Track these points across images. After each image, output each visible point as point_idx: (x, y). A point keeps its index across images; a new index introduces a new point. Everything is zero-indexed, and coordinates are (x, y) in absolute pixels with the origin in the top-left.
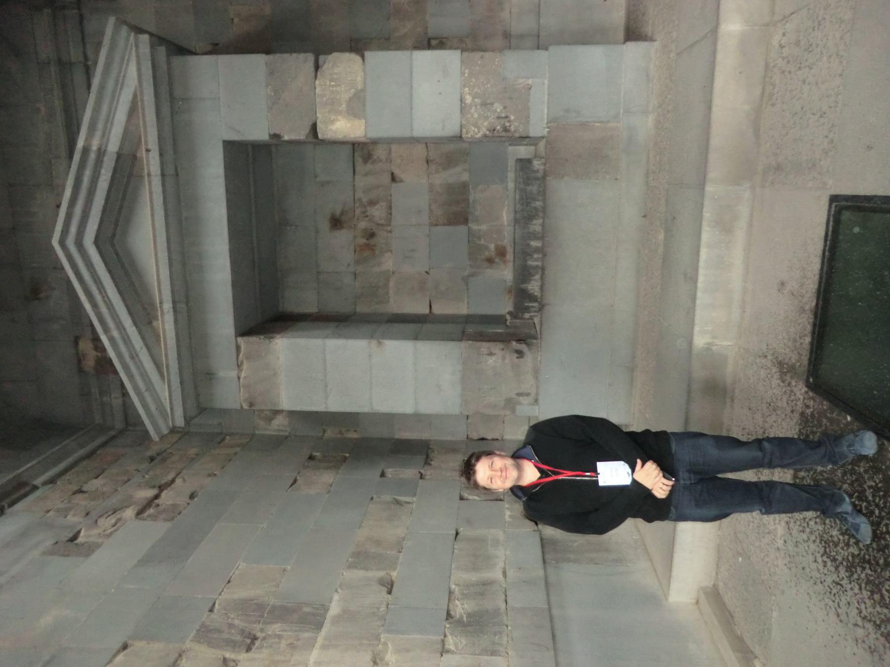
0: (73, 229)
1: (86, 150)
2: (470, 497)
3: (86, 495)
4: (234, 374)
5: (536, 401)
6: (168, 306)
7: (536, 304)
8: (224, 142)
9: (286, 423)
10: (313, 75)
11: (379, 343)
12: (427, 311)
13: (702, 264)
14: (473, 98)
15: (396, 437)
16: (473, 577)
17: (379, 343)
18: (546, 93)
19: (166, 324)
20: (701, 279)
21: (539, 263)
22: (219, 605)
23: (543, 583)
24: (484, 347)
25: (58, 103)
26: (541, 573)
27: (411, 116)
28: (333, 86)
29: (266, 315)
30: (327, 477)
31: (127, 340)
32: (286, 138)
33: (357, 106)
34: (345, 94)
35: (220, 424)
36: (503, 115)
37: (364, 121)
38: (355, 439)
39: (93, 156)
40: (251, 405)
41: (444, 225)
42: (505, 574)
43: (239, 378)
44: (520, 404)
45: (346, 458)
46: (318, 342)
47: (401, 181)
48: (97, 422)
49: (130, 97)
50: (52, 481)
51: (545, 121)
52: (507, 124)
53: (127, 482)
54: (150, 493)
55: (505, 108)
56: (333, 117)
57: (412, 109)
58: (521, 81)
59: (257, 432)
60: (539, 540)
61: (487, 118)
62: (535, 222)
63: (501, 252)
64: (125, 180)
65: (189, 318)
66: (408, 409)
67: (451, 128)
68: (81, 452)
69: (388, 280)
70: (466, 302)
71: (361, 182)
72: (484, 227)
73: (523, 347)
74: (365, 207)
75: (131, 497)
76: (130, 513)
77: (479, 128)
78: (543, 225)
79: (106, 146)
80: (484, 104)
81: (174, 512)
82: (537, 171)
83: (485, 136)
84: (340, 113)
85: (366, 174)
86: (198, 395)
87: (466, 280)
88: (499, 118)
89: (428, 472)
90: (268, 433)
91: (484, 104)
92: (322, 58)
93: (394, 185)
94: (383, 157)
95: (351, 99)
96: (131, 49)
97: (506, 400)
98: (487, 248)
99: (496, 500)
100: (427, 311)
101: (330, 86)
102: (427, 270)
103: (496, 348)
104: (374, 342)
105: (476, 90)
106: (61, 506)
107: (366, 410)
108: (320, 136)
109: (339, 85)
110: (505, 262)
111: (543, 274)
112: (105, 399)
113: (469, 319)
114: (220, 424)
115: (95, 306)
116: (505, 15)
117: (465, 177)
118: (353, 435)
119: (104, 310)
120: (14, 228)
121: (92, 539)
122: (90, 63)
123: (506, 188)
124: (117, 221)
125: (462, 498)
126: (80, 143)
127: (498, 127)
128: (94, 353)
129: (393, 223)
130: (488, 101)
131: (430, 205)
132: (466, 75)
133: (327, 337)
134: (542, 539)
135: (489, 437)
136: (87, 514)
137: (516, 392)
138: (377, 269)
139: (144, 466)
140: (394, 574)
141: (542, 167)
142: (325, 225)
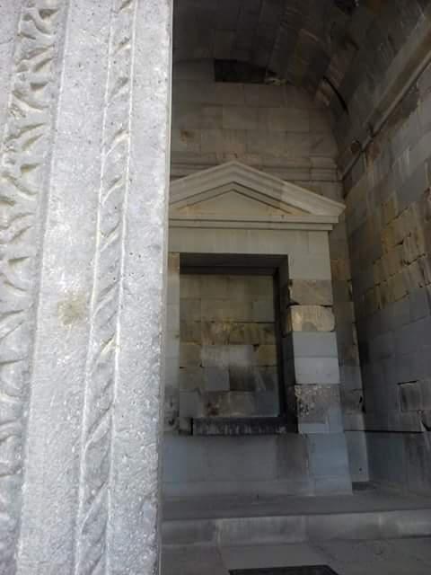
1: (283, 185)
6: (200, 217)
8: (285, 258)
11: (177, 337)
17: (177, 337)
20: (255, 519)
21: (226, 433)
34: (314, 321)
39: (279, 187)
47: (255, 350)
61: (306, 398)
63: (214, 412)
67: (299, 379)
69: (195, 341)
78: (248, 434)
80: (313, 397)
83: (296, 398)
84: (304, 318)
87: (197, 390)
98: (217, 402)
104: (178, 334)
108: (292, 307)
110: (209, 415)
115: (200, 177)
117: (259, 389)
126: (286, 183)
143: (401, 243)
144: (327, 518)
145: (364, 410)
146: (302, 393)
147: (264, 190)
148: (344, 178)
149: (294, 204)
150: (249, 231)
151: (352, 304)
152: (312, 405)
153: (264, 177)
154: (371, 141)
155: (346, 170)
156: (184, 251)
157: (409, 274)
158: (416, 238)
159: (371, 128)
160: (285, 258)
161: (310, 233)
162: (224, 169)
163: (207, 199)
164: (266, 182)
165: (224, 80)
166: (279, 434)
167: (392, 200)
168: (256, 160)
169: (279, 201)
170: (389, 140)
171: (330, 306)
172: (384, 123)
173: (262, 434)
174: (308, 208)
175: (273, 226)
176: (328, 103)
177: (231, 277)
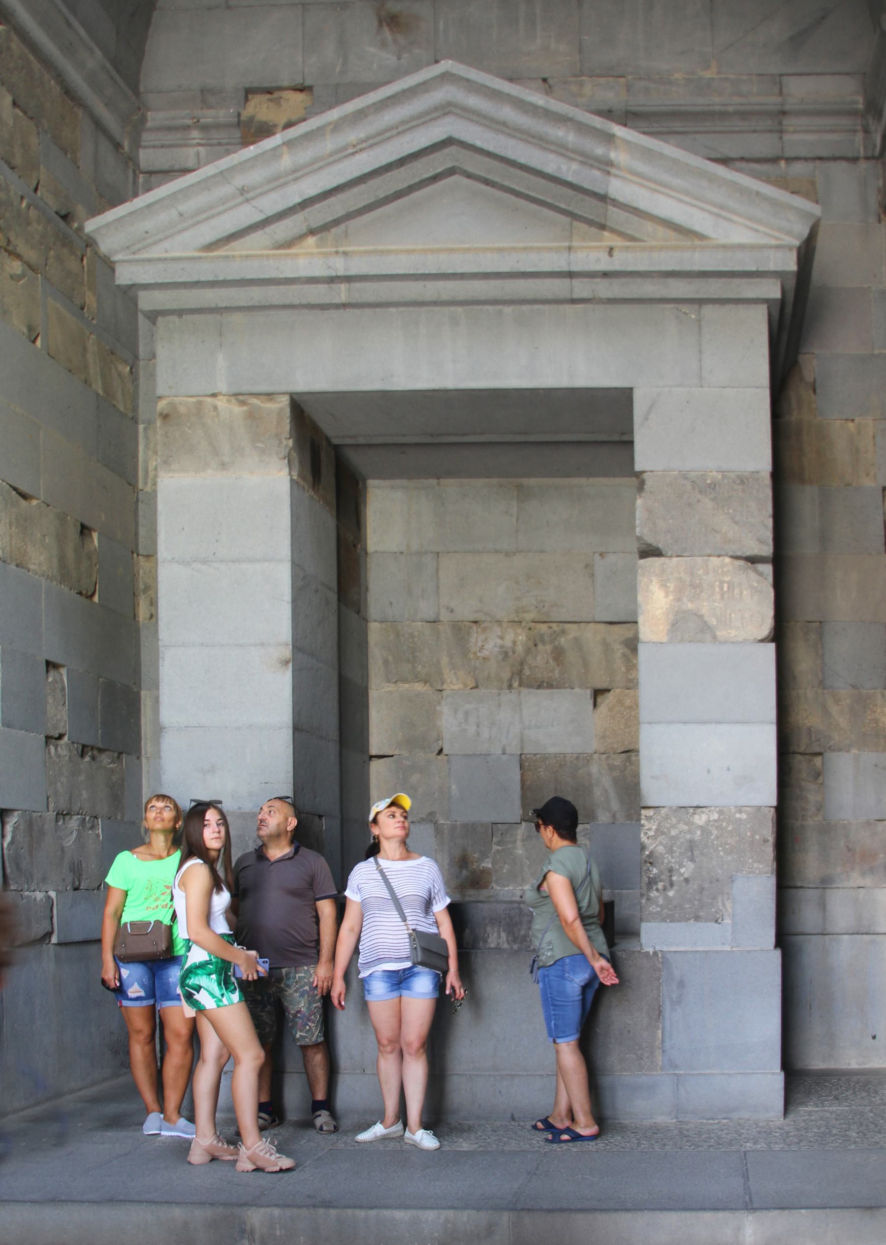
14: (703, 829)
80: (691, 845)
146: (659, 832)
150: (508, 310)
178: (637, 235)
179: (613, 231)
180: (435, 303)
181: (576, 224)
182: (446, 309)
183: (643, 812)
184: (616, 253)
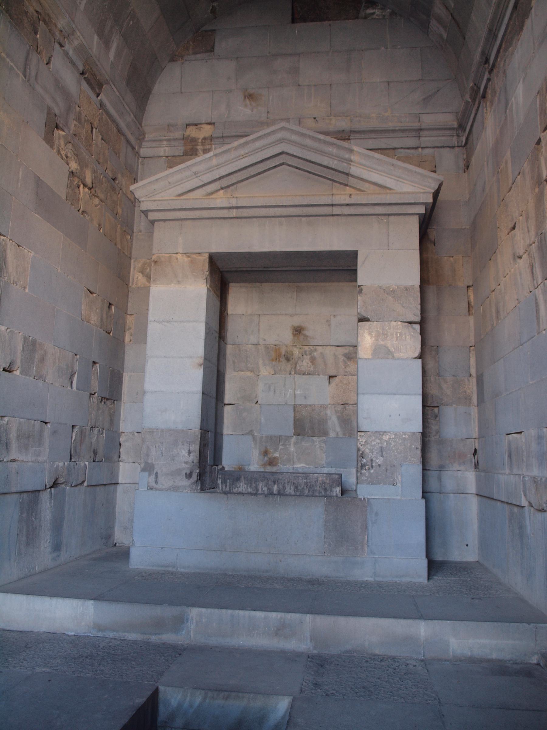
0: (294, 137)
1: (351, 151)
2: (74, 434)
3: (90, 131)
4: (180, 250)
5: (151, 489)
6: (234, 203)
7: (228, 489)
8: (357, 251)
9: (139, 285)
10: (405, 320)
11: (201, 365)
12: (226, 402)
13: (253, 613)
15: (124, 374)
16: (13, 435)
17: (201, 365)
18: (389, 498)
19: (221, 200)
20: (241, 613)
22: (3, 240)
23: (6, 491)
24: (196, 447)
25: (390, 125)
26: (14, 490)
27: (374, 394)
28: (397, 335)
29: (225, 274)
30: (95, 319)
31: (209, 170)
32: (359, 297)
33: (381, 352)
34: (390, 343)
35: (140, 231)
36: (373, 464)
37: (370, 357)
38: (124, 341)
39: (347, 156)
40: (155, 262)
41: (295, 417)
42: (14, 460)
43: (176, 253)
44: (149, 475)
45: (109, 333)
46: (203, 317)
48: (146, 135)
49: (388, 186)
50: (102, 105)
51: (369, 497)
52: (367, 467)
53: (98, 162)
54: (89, 181)
55: (379, 465)
56: (374, 334)
57: (379, 394)
58: (399, 477)
59: (132, 261)
60: (39, 489)
62: (293, 488)
64: (329, 177)
65: (225, 218)
66: (148, 387)
67: (364, 425)
68: (123, 125)
70: (233, 433)
71: (329, 352)
72: (292, 449)
73: (195, 477)
74: (310, 354)
75: (87, 166)
76: (74, 166)
77: (364, 445)
78: (290, 495)
79: (353, 165)
80: (382, 449)
81: (73, 199)
82: (331, 491)
83: (359, 450)
85: (335, 356)
86: (164, 221)
87: (251, 433)
88: (372, 460)
89: (95, 399)
90: (132, 269)
91: (382, 449)
92: (417, 327)
93: (327, 377)
94: (348, 369)
95: (387, 348)
96: (423, 189)
97: (153, 465)
98: (276, 450)
99: (71, 455)
100: (226, 402)
101: (397, 333)
102: (259, 402)
103: (194, 457)
104: (202, 361)
105: (393, 444)
106: (83, 115)
107: (148, 353)
109: (397, 339)
110: (264, 465)
111: (251, 494)
112: (165, 143)
113: (218, 435)
114: (140, 231)
115: (236, 148)
116: (456, 467)
117: (332, 434)
118: (127, 339)
119: (233, 155)
120: (299, 85)
121: (57, 141)
122: (420, 150)
123: (324, 467)
124: (300, 169)
125: (73, 427)
127: (364, 461)
128: (201, 136)
129: (297, 376)
130: (384, 453)
131: (310, 405)
132: (404, 436)
133: (207, 323)
134: (39, 491)
135: (122, 450)
136: (75, 135)
137: (159, 472)
138: (261, 362)
139: (110, 175)
140: (18, 373)
141: (334, 494)
142: (297, 321)
143: (514, 228)
144: (342, 621)
145: (476, 466)
147: (326, 161)
148: (466, 143)
149: (370, 179)
150: (304, 219)
151: (471, 319)
152: (380, 460)
153: (325, 142)
154: (489, 80)
155: (467, 130)
156: (214, 249)
157: (520, 274)
158: (527, 218)
159: (487, 61)
160: (353, 255)
161: (392, 218)
162: (274, 132)
163: (247, 179)
164: (330, 149)
165: (304, 20)
166: (331, 497)
167: (506, 162)
168: (343, 124)
169: (348, 174)
170: (505, 73)
171: (415, 323)
172: (500, 46)
173: (307, 496)
174: (389, 182)
175: (336, 210)
176: (445, 36)
177: (303, 284)
178: (362, 189)
179: (350, 186)
180: (273, 217)
181: (334, 184)
182: (277, 219)
183: (359, 433)
184: (352, 196)
